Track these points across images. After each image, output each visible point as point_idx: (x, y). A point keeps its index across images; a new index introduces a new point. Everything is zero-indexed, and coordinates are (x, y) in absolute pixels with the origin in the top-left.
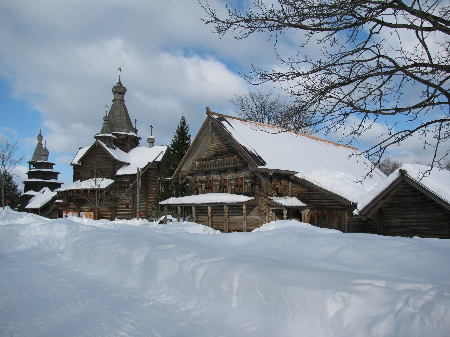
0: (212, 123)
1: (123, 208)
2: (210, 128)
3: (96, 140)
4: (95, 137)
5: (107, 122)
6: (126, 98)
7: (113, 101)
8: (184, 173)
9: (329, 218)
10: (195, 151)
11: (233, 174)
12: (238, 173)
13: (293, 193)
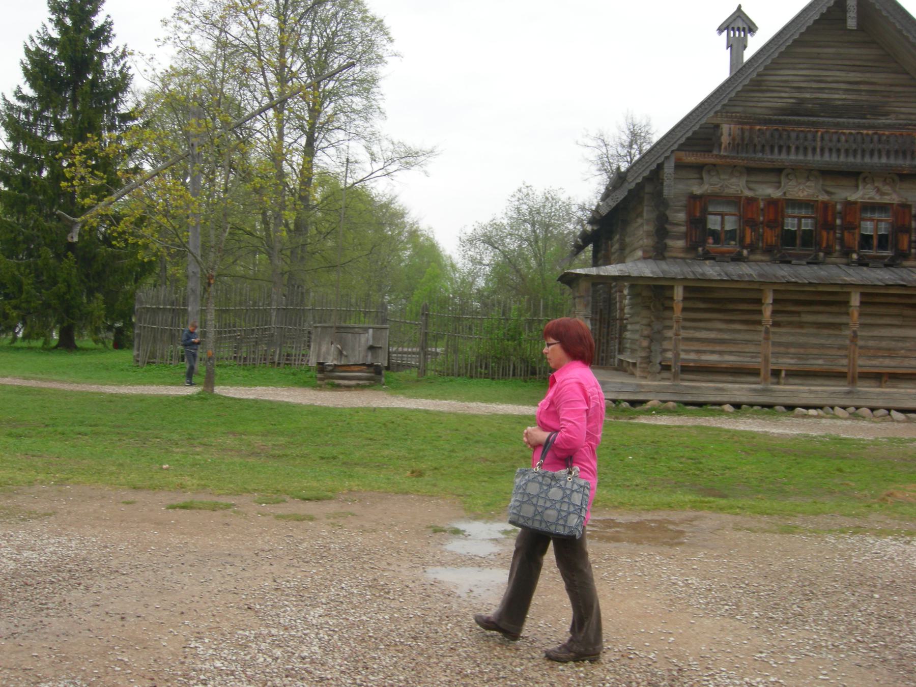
11: (886, 189)
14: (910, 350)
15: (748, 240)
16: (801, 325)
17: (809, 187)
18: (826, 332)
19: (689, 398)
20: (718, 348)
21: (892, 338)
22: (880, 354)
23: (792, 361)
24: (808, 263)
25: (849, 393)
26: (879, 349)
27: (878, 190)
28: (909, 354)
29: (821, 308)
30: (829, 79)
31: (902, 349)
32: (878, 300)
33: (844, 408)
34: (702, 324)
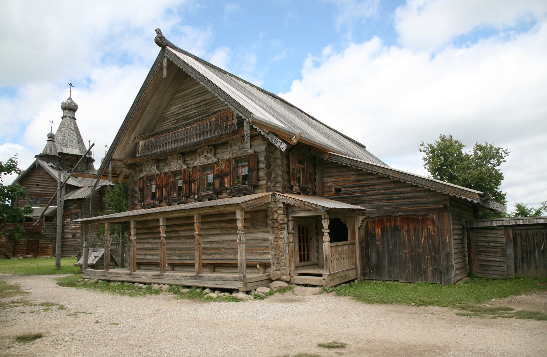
0: (168, 60)
1: (69, 238)
2: (165, 70)
3: (36, 159)
4: (36, 156)
5: (51, 139)
6: (77, 115)
7: (62, 118)
8: (119, 163)
9: (408, 231)
11: (209, 155)
12: (218, 151)
13: (323, 187)
14: (227, 249)
15: (157, 196)
16: (179, 238)
17: (178, 164)
19: (108, 278)
20: (152, 252)
21: (218, 242)
22: (213, 252)
23: (177, 258)
24: (178, 204)
25: (160, 275)
26: (213, 249)
29: (186, 228)
30: (189, 105)
31: (223, 248)
33: (159, 284)
34: (146, 241)
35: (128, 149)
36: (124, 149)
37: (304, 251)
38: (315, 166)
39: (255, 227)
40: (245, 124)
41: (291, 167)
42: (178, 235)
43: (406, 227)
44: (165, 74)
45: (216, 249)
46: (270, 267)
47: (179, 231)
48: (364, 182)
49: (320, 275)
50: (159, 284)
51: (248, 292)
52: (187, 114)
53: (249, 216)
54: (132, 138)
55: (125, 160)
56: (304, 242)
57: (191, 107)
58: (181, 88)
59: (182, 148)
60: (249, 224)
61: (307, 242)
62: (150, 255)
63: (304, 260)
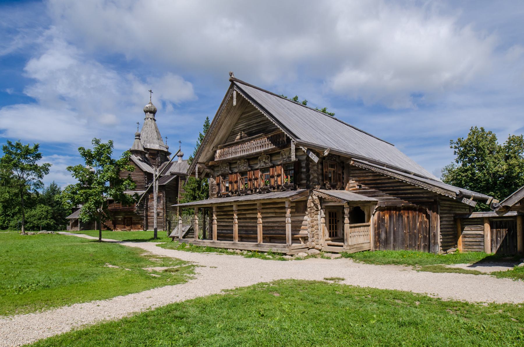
0: (237, 92)
10: (216, 135)
11: (267, 161)
16: (246, 218)
18: (252, 221)
20: (226, 228)
27: (264, 162)
28: (278, 228)
32: (267, 206)
33: (233, 249)
34: (222, 220)
35: (209, 155)
36: (206, 155)
37: (333, 230)
38: (343, 168)
39: (298, 212)
40: (292, 143)
41: (324, 171)
42: (244, 216)
43: (406, 215)
44: (235, 103)
45: (272, 227)
46: (308, 240)
47: (245, 214)
48: (378, 181)
49: (342, 246)
50: (233, 249)
51: (292, 255)
52: (250, 130)
53: (294, 205)
54: (212, 148)
55: (207, 163)
56: (333, 223)
57: (253, 126)
58: (247, 110)
59: (247, 156)
60: (294, 210)
61: (336, 223)
62: (225, 230)
63: (333, 236)
